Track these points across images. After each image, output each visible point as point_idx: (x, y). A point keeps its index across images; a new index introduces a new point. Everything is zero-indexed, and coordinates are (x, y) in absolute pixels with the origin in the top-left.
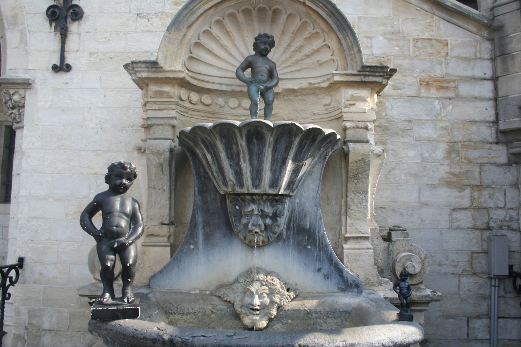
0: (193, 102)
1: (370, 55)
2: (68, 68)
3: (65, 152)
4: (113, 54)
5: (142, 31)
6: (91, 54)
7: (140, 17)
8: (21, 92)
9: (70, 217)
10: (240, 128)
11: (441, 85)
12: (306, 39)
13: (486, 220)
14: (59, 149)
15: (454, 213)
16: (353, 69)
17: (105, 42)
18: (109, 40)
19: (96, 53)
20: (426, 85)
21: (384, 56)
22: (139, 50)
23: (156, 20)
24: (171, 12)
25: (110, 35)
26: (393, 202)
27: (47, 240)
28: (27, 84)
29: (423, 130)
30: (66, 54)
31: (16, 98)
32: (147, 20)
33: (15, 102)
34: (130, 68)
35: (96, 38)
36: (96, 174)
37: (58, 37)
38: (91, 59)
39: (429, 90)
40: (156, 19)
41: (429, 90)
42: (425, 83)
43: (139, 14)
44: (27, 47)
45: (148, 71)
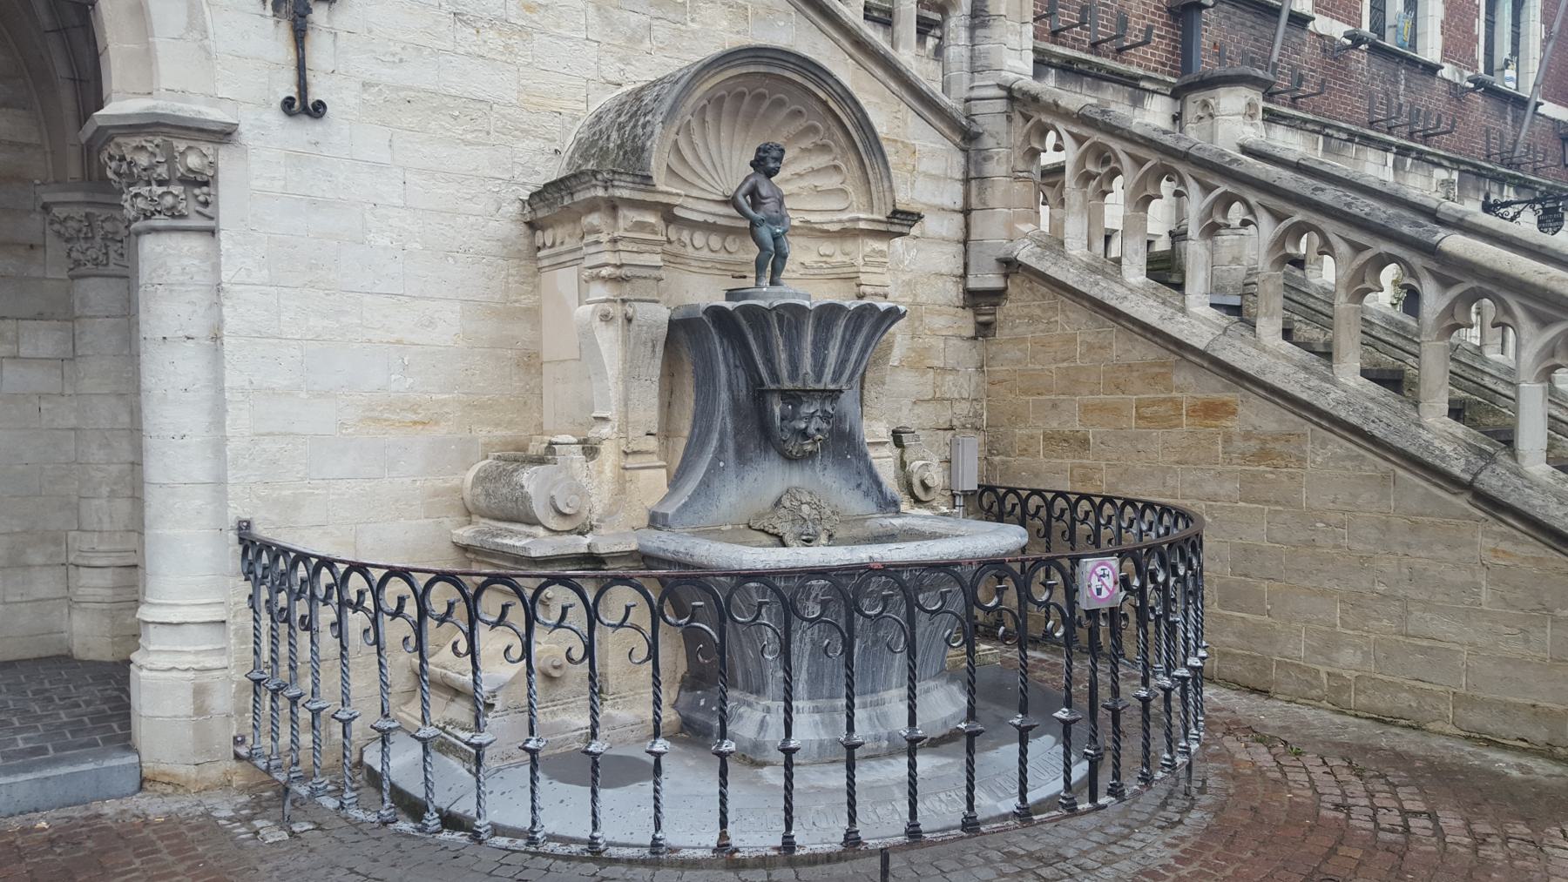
2: (317, 110)
3: (327, 294)
4: (412, 94)
5: (468, 54)
6: (366, 85)
7: (460, 20)
8: (207, 148)
9: (350, 430)
12: (803, 150)
13: (949, 417)
14: (313, 287)
15: (916, 407)
16: (880, 213)
17: (394, 62)
18: (401, 60)
19: (377, 85)
22: (466, 95)
23: (492, 34)
24: (521, 22)
25: (403, 49)
27: (302, 479)
28: (224, 135)
30: (309, 76)
31: (193, 161)
33: (190, 170)
35: (374, 51)
36: (399, 342)
37: (285, 30)
38: (365, 96)
44: (206, 42)
45: (632, 189)
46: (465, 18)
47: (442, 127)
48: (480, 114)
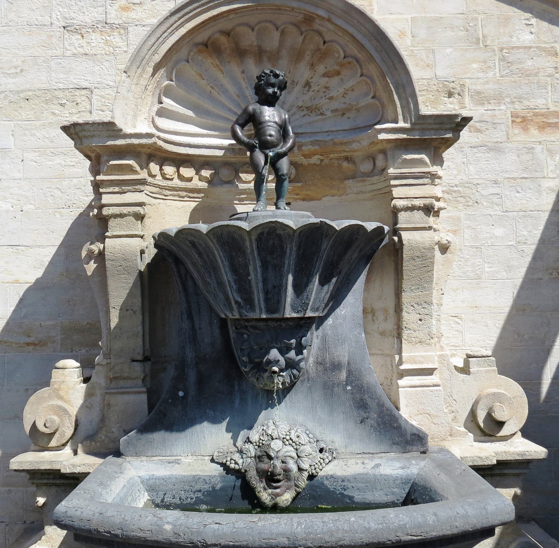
0: (167, 176)
1: (431, 79)
4: (30, 93)
5: (75, 55)
10: (249, 233)
11: (545, 120)
18: (22, 71)
20: (521, 122)
21: (454, 79)
26: (472, 307)
29: (517, 194)
32: (80, 37)
34: (72, 131)
39: (525, 129)
40: (94, 34)
41: (525, 129)
42: (519, 120)
43: (67, 27)
46: (72, 29)
47: (54, 114)
48: (84, 98)
